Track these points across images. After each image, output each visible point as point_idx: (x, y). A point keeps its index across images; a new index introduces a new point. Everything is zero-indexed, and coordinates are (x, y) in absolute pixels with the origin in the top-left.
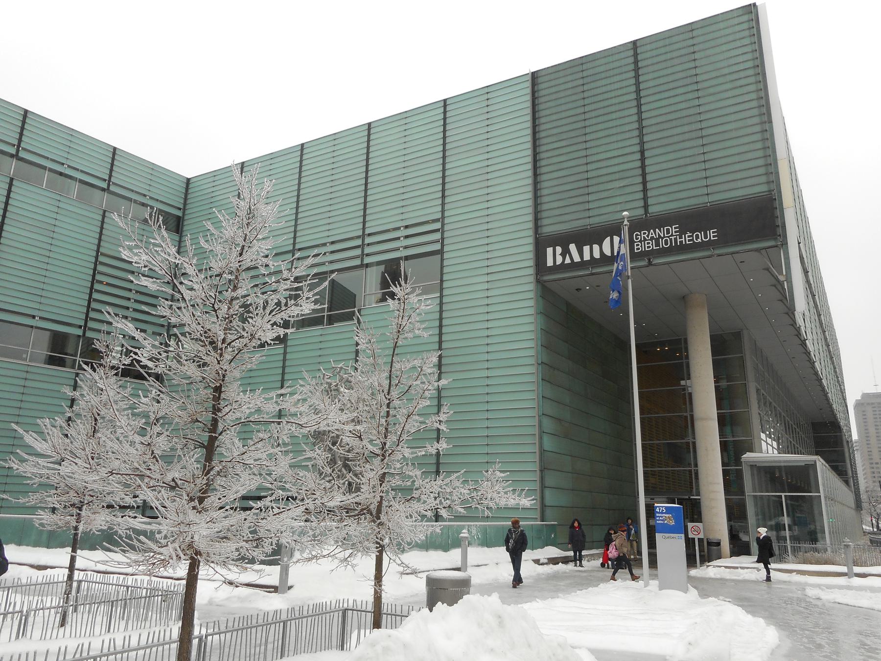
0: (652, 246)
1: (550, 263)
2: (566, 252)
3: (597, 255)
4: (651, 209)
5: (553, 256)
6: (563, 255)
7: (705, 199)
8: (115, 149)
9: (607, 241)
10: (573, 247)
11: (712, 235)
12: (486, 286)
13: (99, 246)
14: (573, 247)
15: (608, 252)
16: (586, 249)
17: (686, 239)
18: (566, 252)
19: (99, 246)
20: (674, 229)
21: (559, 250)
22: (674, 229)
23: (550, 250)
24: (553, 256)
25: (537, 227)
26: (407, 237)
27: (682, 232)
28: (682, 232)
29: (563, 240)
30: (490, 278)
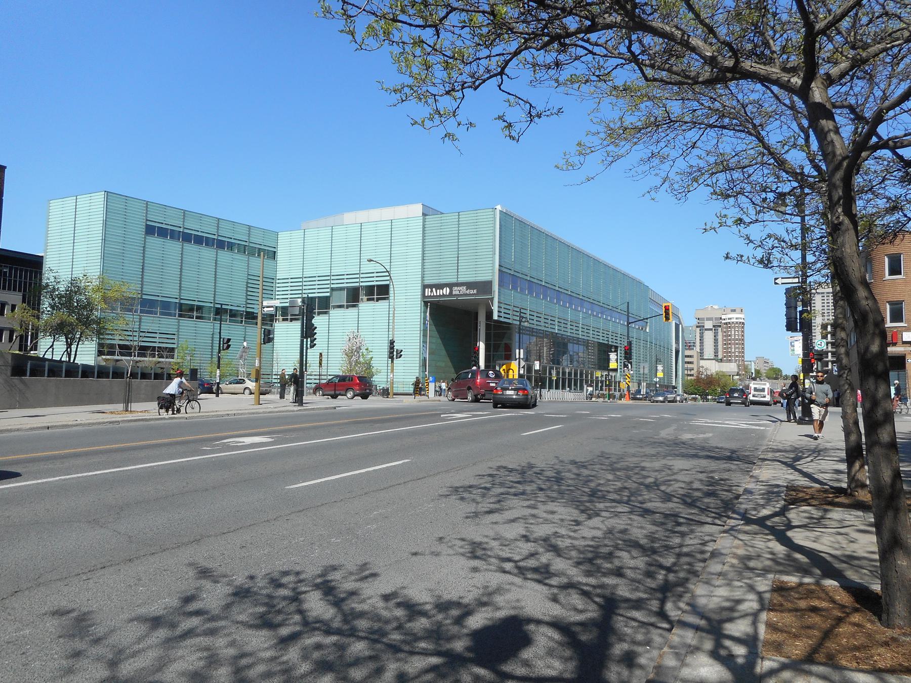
0: (458, 293)
1: (426, 295)
2: (432, 291)
3: (441, 294)
4: (459, 279)
5: (428, 292)
6: (431, 292)
7: (475, 278)
8: (250, 227)
9: (445, 289)
10: (434, 289)
11: (475, 291)
12: (405, 300)
13: (248, 272)
14: (434, 289)
15: (445, 293)
16: (438, 291)
17: (468, 292)
18: (432, 291)
19: (248, 272)
20: (465, 288)
21: (430, 290)
22: (465, 288)
23: (427, 290)
24: (428, 292)
25: (423, 280)
26: (377, 277)
27: (467, 290)
28: (467, 290)
29: (431, 286)
30: (407, 297)
